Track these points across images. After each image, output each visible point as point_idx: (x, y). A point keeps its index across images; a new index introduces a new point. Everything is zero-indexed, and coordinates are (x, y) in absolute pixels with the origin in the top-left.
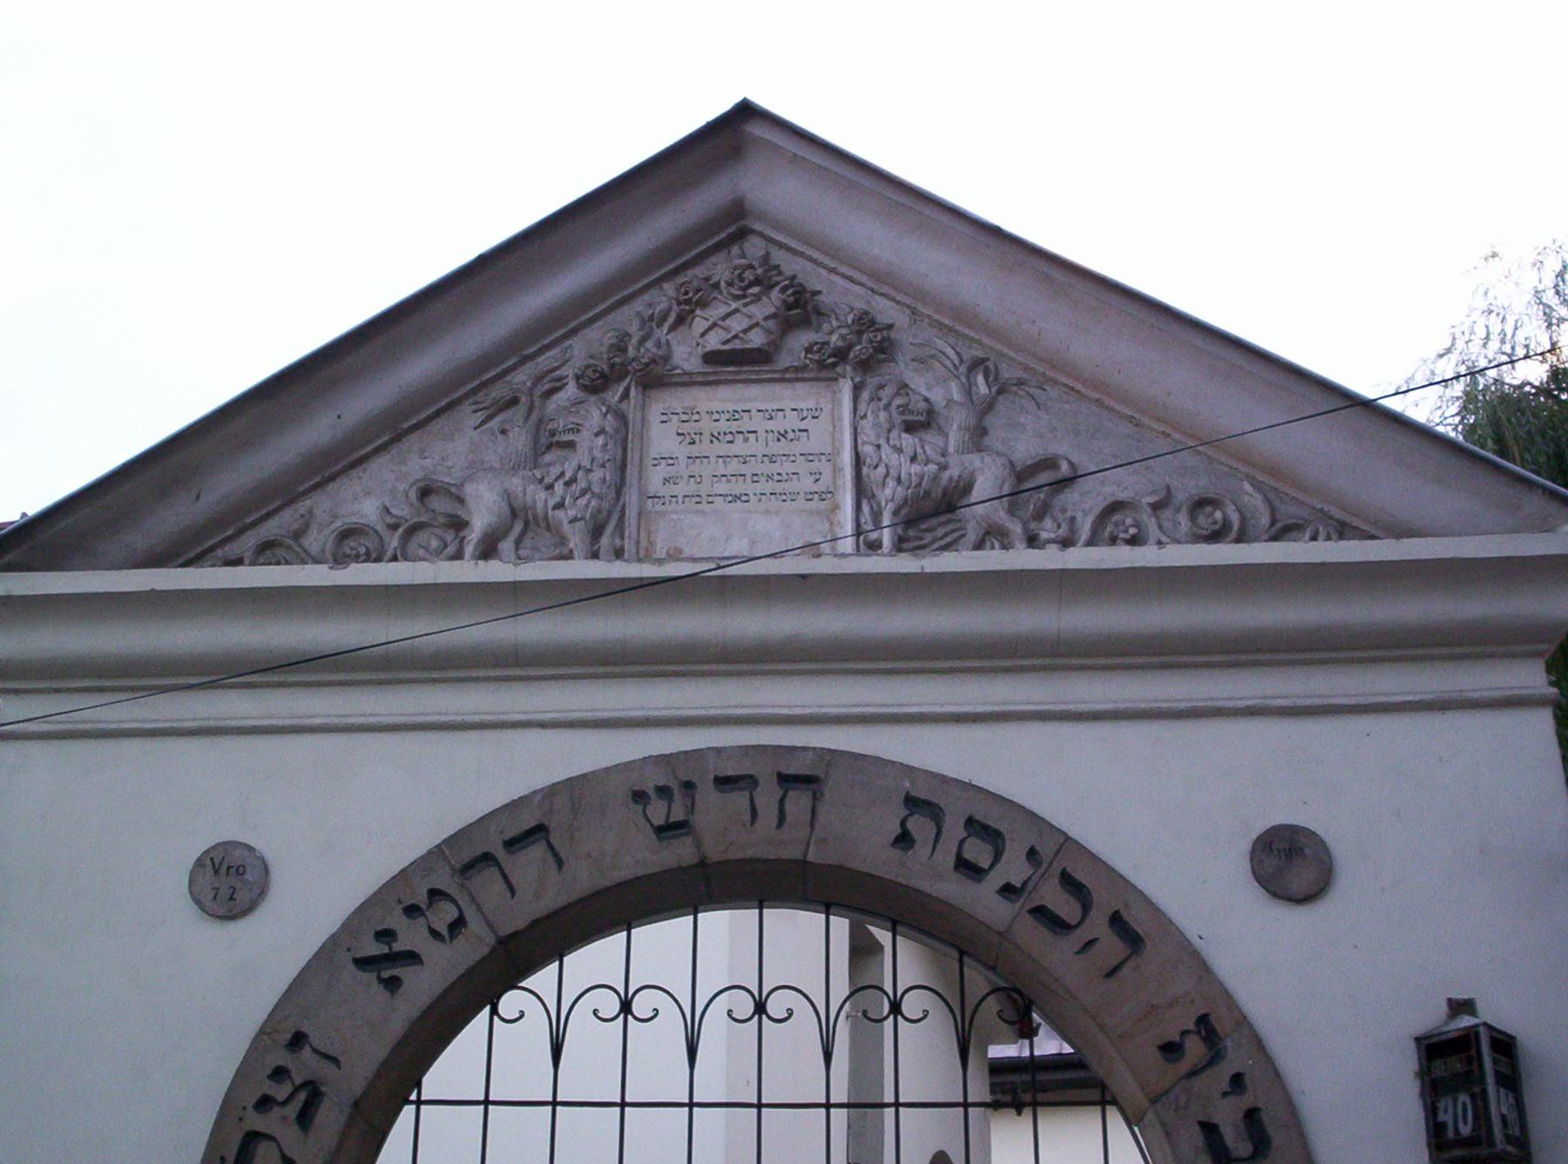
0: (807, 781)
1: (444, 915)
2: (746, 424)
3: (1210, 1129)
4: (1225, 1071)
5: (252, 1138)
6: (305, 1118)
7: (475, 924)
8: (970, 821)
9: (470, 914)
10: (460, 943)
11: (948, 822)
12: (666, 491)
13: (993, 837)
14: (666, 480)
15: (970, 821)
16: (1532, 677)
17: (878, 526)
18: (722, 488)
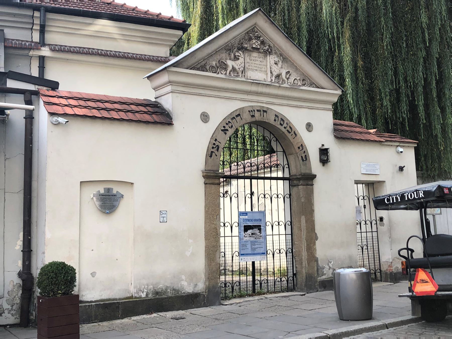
1: (230, 125)
3: (302, 157)
4: (303, 150)
5: (212, 152)
6: (218, 150)
8: (281, 118)
12: (249, 67)
13: (283, 121)
15: (281, 118)
16: (330, 107)
18: (255, 68)
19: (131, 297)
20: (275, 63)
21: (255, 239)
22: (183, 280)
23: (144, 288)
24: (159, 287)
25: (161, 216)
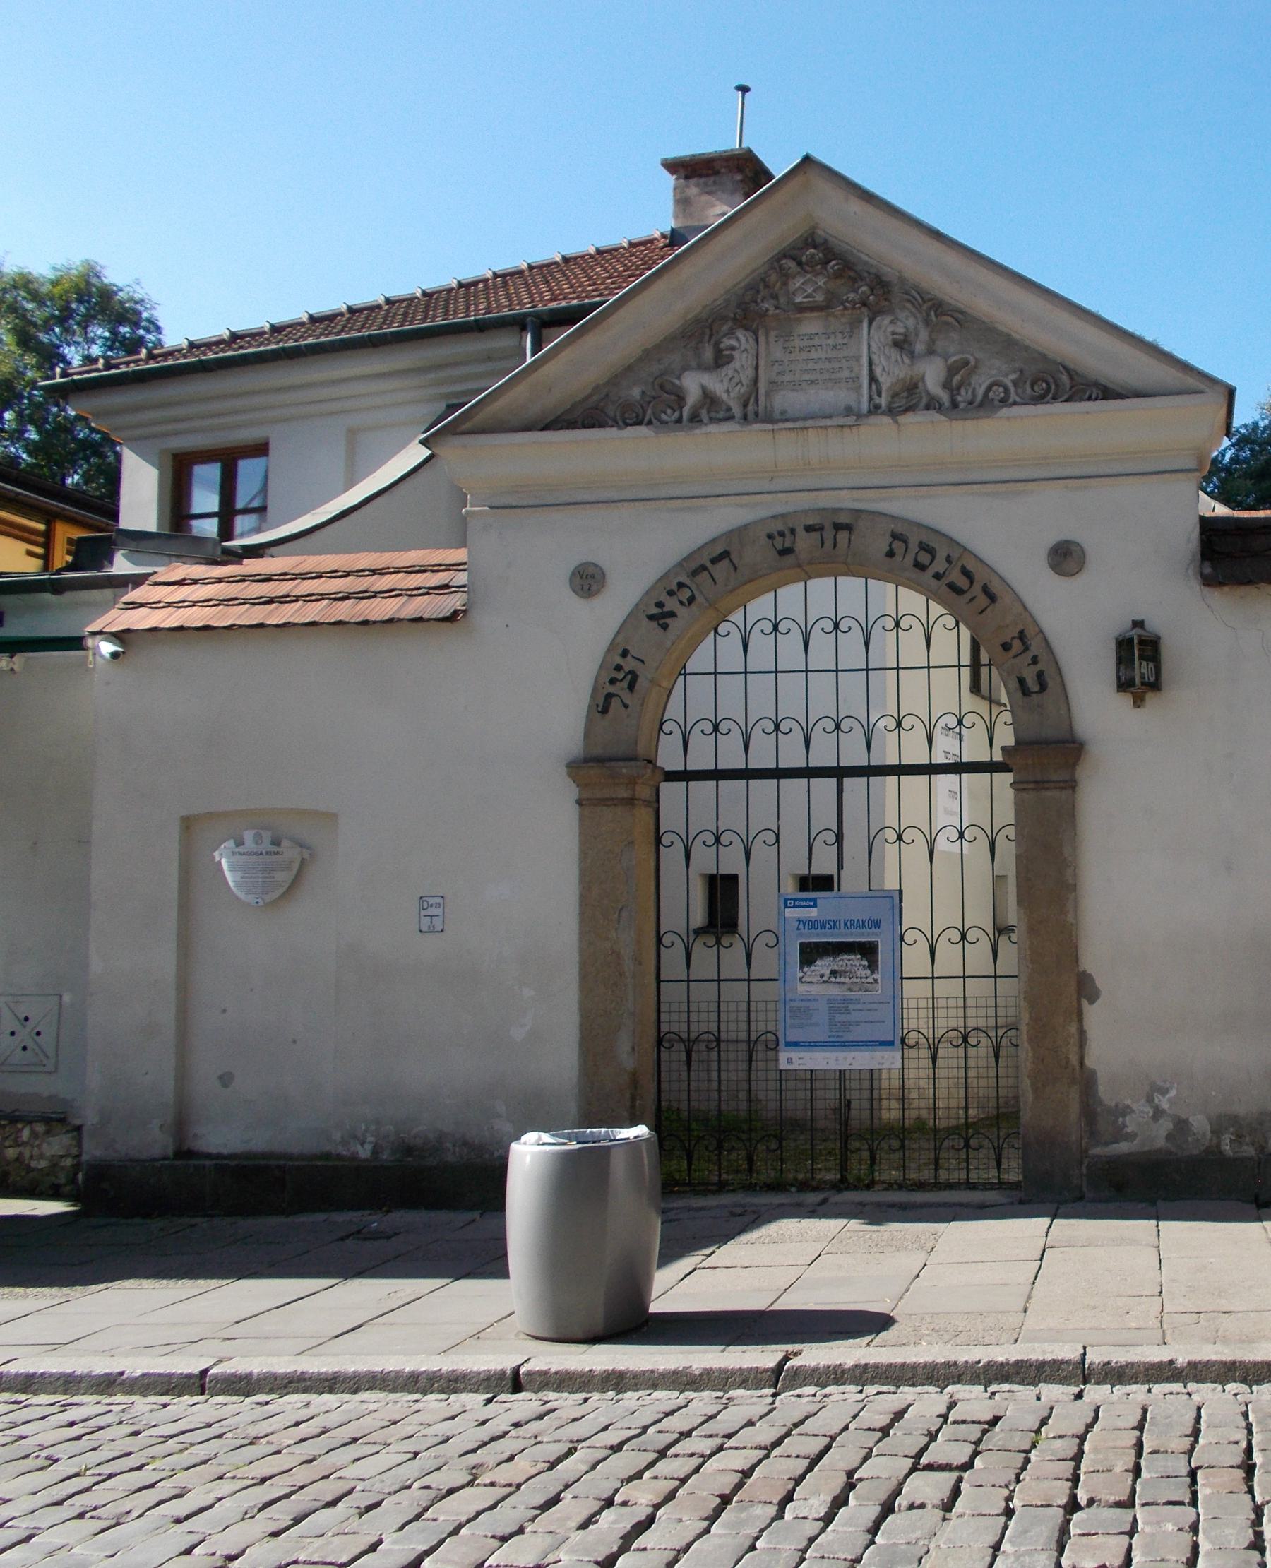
0: (848, 527)
2: (816, 342)
3: (1021, 681)
4: (1030, 654)
6: (631, 687)
7: (700, 599)
9: (697, 594)
10: (694, 607)
11: (911, 546)
12: (780, 379)
13: (931, 551)
14: (779, 373)
17: (879, 395)
18: (806, 377)
19: (327, 1156)
20: (896, 344)
21: (850, 990)
22: (500, 1116)
23: (366, 1131)
24: (414, 1131)
25: (424, 913)
